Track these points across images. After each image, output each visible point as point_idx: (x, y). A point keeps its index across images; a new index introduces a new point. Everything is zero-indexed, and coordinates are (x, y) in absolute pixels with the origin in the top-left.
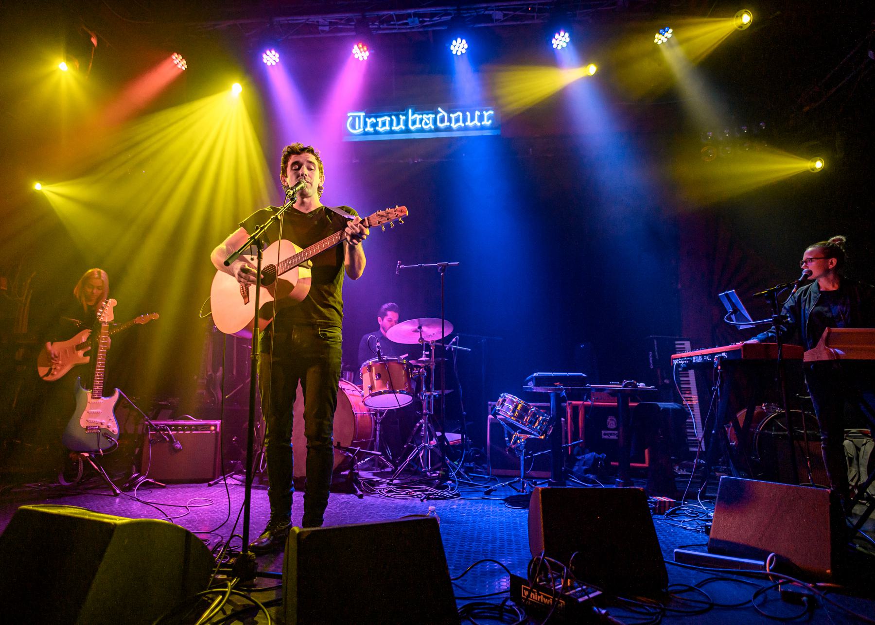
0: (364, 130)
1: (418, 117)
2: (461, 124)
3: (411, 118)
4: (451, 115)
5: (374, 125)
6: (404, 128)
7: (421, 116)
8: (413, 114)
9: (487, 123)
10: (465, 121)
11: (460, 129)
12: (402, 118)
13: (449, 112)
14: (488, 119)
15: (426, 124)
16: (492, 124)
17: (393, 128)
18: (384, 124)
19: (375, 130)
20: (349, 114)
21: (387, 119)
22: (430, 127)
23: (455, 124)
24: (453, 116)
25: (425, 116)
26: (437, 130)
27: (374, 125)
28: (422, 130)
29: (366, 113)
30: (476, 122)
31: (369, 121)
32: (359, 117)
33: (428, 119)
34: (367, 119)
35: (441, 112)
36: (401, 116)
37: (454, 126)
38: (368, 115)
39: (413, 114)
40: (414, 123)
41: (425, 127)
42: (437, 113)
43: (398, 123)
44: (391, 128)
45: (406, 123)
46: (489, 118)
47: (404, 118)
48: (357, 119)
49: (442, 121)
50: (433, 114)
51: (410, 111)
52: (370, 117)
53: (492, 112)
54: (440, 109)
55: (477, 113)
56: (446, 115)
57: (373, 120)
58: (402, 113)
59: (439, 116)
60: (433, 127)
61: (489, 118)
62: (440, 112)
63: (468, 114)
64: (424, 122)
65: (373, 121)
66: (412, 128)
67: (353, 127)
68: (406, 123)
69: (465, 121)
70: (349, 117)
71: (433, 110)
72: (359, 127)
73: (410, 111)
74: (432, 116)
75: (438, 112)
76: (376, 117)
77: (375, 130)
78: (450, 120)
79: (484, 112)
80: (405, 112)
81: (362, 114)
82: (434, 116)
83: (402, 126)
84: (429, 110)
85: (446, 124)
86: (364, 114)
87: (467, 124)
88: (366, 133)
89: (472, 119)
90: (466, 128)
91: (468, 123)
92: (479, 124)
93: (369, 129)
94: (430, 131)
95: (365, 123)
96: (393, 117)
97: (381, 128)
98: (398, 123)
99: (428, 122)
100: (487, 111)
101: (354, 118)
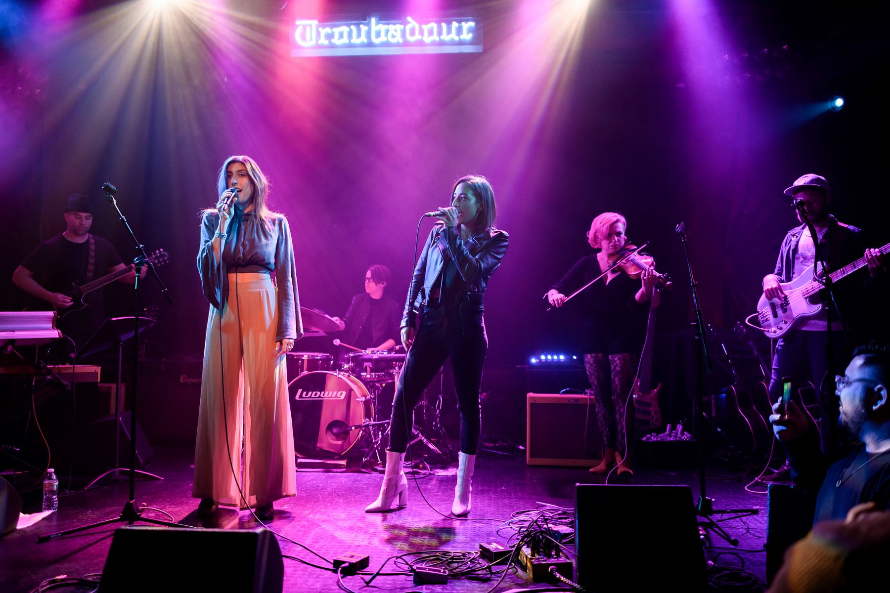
0: (317, 42)
1: (382, 27)
2: (435, 38)
4: (424, 26)
5: (330, 37)
6: (365, 41)
7: (386, 27)
8: (377, 23)
9: (467, 36)
11: (434, 44)
13: (421, 23)
14: (468, 33)
15: (393, 36)
16: (474, 37)
17: (352, 41)
18: (341, 35)
19: (330, 42)
21: (345, 29)
22: (398, 41)
23: (428, 37)
24: (426, 28)
26: (406, 44)
27: (330, 37)
28: (387, 44)
29: (320, 21)
30: (454, 36)
32: (311, 26)
34: (321, 29)
35: (411, 23)
36: (362, 26)
37: (427, 39)
39: (377, 23)
40: (378, 34)
41: (393, 41)
42: (405, 23)
43: (359, 35)
44: (350, 40)
45: (369, 33)
48: (308, 28)
49: (413, 33)
50: (401, 24)
51: (373, 20)
52: (324, 27)
53: (472, 24)
54: (409, 19)
55: (455, 25)
57: (328, 30)
59: (408, 27)
60: (401, 41)
62: (410, 23)
63: (444, 25)
64: (390, 34)
67: (303, 37)
68: (369, 33)
70: (297, 26)
72: (311, 39)
73: (373, 20)
74: (399, 27)
75: (408, 23)
76: (332, 27)
77: (330, 42)
78: (422, 33)
80: (367, 21)
82: (402, 27)
83: (363, 39)
85: (417, 37)
87: (442, 37)
89: (449, 32)
90: (442, 43)
91: (445, 37)
92: (457, 38)
93: (324, 41)
94: (398, 45)
95: (318, 33)
96: (353, 27)
97: (338, 40)
98: (359, 35)
99: (395, 34)
100: (467, 21)
101: (304, 27)
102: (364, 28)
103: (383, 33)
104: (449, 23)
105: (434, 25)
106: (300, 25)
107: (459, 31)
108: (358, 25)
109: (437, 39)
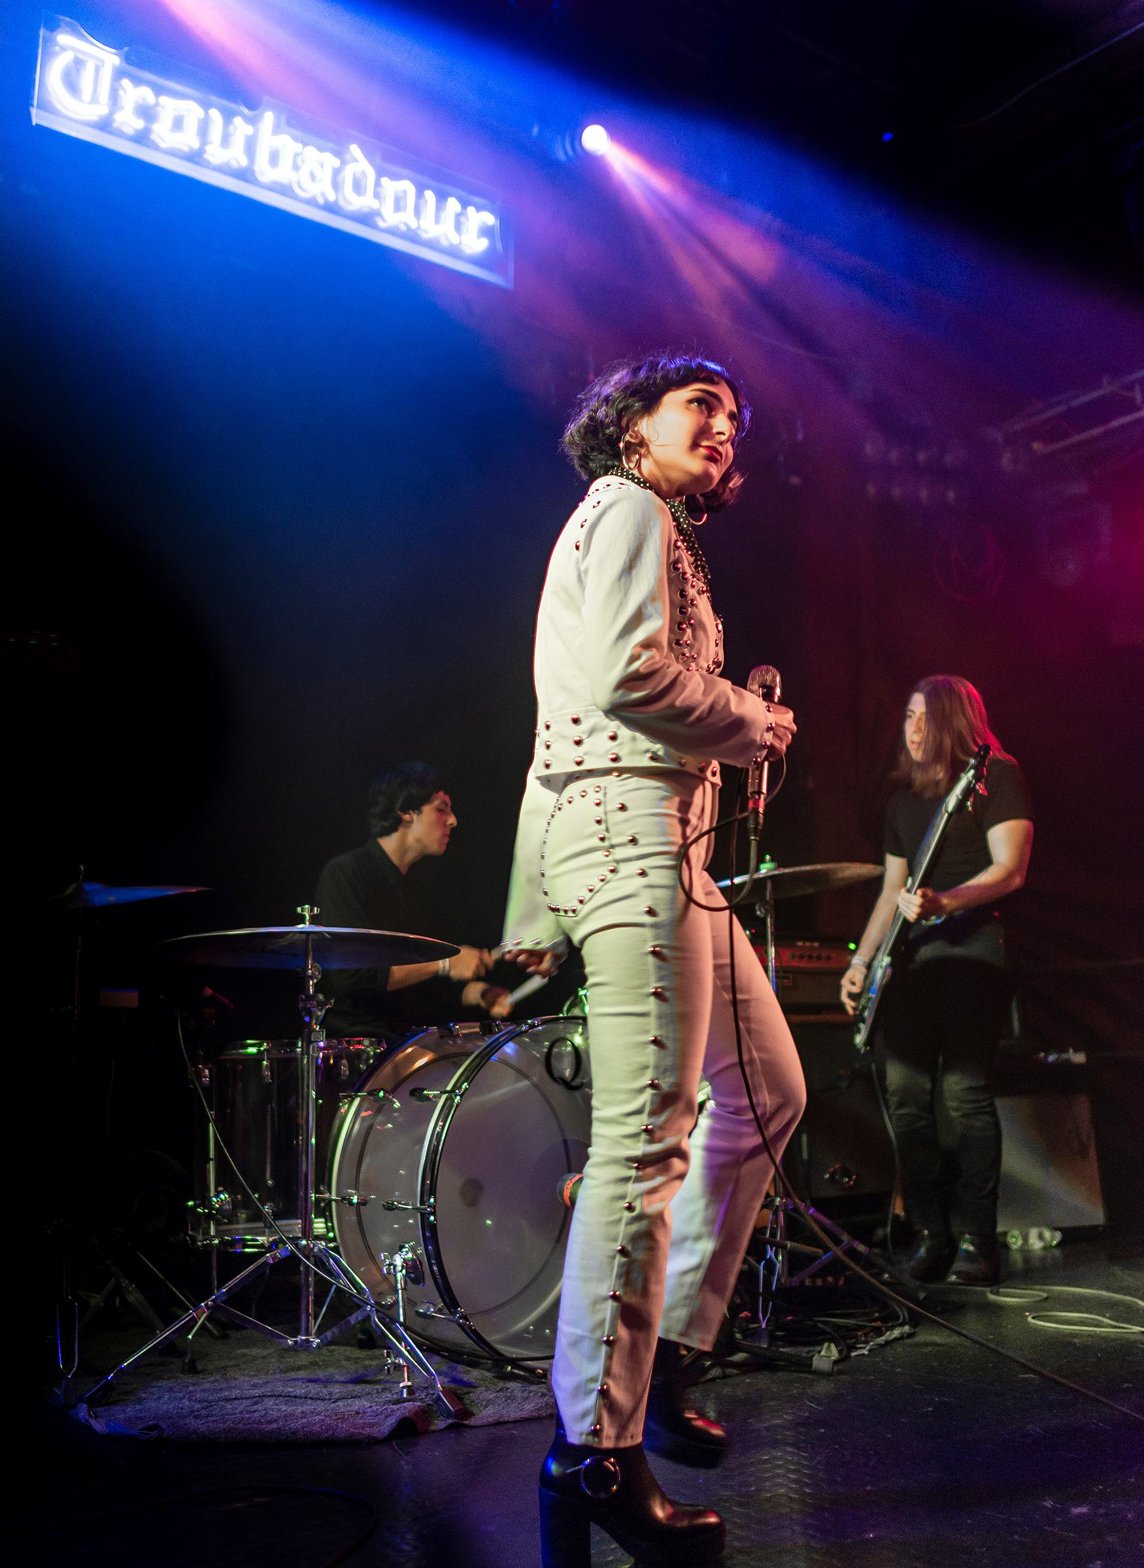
1: (287, 144)
2: (405, 219)
4: (385, 181)
5: (147, 113)
7: (298, 147)
8: (277, 130)
9: (477, 245)
10: (418, 212)
13: (380, 173)
15: (313, 177)
18: (178, 124)
20: (64, 38)
21: (191, 110)
25: (311, 151)
27: (147, 113)
29: (127, 59)
31: (134, 94)
33: (322, 166)
34: (126, 83)
35: (356, 160)
38: (132, 69)
40: (274, 159)
43: (226, 140)
45: (250, 147)
46: (486, 232)
47: (248, 130)
48: (90, 67)
49: (358, 187)
51: (269, 118)
52: (137, 81)
53: (489, 219)
54: (355, 149)
55: (453, 205)
56: (371, 174)
57: (145, 94)
58: (246, 111)
61: (486, 232)
63: (429, 195)
66: (265, 172)
68: (250, 147)
69: (418, 212)
70: (63, 49)
72: (94, 100)
73: (269, 118)
74: (331, 161)
76: (159, 90)
78: (377, 195)
79: (471, 210)
81: (110, 58)
82: (336, 162)
83: (236, 156)
88: (104, 125)
93: (128, 121)
96: (215, 114)
98: (226, 140)
99: (318, 175)
100: (479, 208)
101: (78, 63)
103: (286, 160)
104: (442, 197)
105: (407, 186)
106: (63, 49)
107: (458, 226)
108: (228, 116)
109: (413, 224)
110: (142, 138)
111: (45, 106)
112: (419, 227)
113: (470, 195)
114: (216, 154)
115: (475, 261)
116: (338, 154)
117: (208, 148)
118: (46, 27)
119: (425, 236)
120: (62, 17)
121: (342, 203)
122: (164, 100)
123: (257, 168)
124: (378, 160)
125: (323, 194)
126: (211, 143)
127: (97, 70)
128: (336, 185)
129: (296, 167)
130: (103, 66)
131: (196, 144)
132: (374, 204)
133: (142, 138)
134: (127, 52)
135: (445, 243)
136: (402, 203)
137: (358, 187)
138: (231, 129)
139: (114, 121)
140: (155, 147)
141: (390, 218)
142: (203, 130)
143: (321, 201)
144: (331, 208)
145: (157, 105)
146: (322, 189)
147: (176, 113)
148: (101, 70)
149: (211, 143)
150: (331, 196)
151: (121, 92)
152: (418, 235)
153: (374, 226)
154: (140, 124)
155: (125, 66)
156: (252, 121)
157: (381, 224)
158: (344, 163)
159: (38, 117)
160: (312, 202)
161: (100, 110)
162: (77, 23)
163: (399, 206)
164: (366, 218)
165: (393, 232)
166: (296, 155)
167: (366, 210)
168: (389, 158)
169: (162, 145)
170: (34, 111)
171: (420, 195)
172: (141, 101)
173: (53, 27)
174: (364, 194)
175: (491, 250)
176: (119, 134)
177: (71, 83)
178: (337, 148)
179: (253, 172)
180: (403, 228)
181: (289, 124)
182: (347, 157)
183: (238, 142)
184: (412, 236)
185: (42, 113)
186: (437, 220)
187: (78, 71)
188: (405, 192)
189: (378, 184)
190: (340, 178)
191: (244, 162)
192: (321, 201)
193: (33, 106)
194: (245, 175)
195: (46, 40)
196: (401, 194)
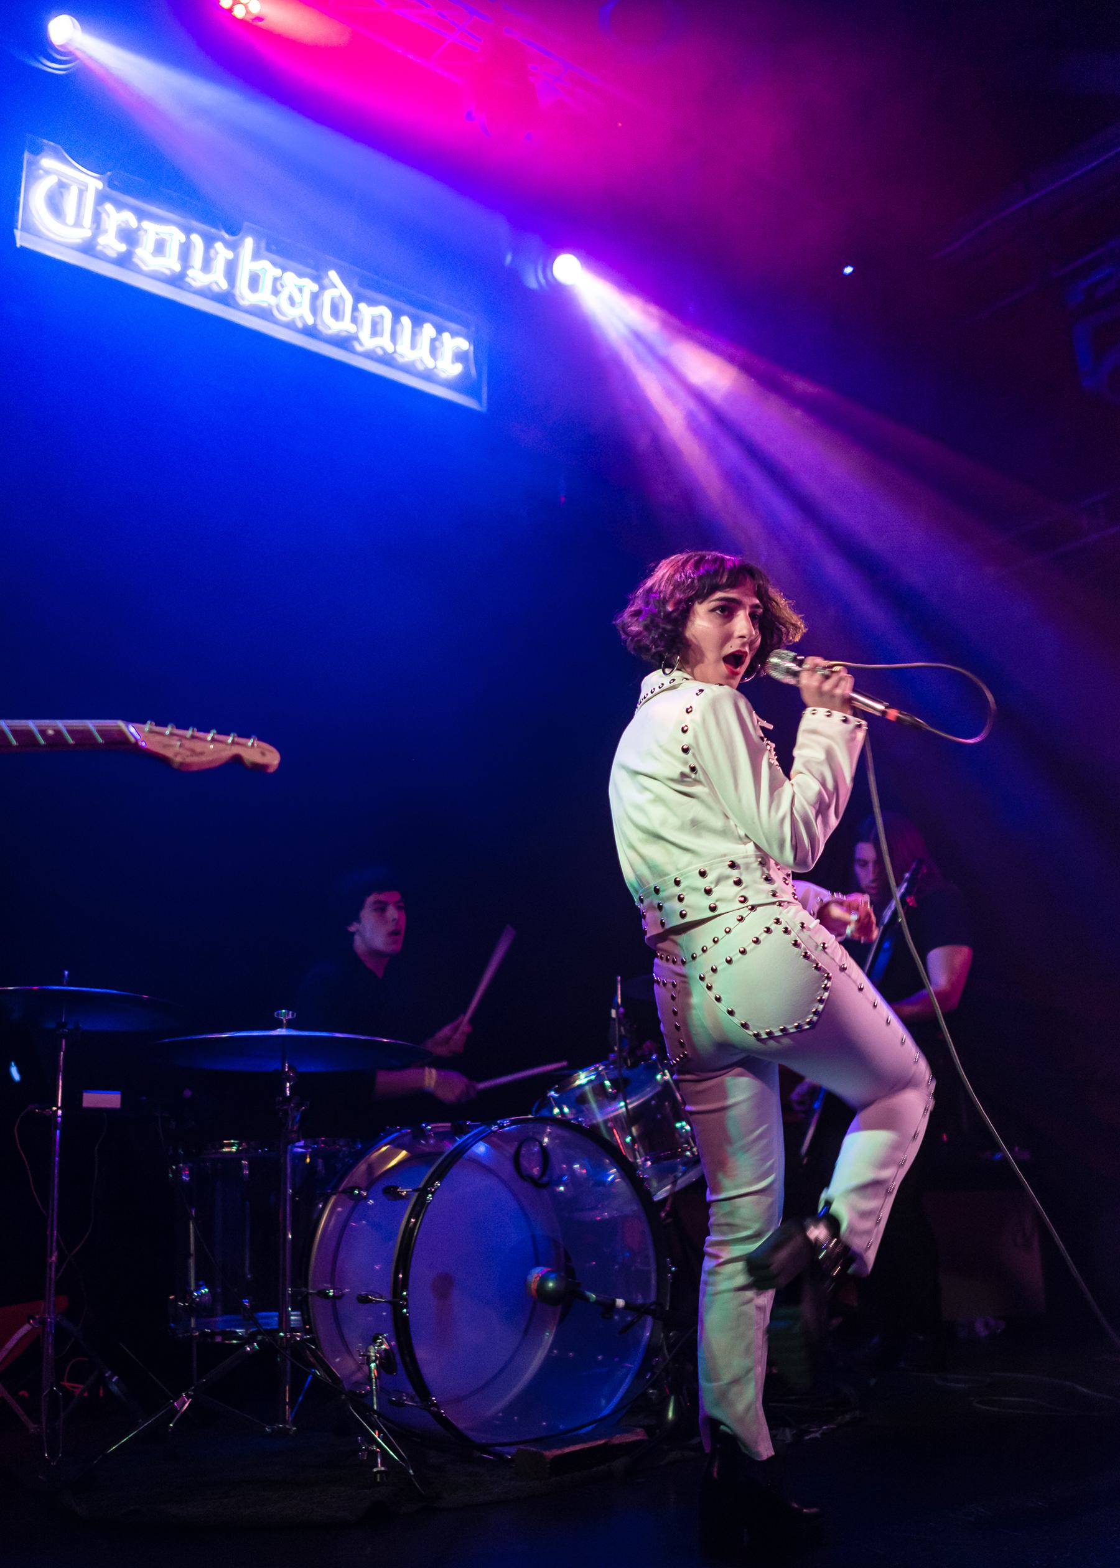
1: (267, 269)
2: (383, 343)
3: (247, 265)
4: (362, 306)
5: (129, 237)
7: (278, 272)
8: (256, 256)
9: (451, 369)
12: (222, 253)
13: (358, 298)
15: (292, 301)
18: (160, 248)
20: (47, 162)
21: (174, 235)
24: (367, 312)
27: (129, 237)
29: (110, 184)
31: (117, 218)
33: (300, 290)
34: (109, 207)
35: (335, 287)
36: (219, 246)
40: (254, 282)
43: (207, 266)
46: (460, 357)
47: (230, 255)
48: (74, 191)
49: (336, 312)
51: (249, 243)
52: (120, 206)
53: (464, 344)
54: (333, 275)
55: (428, 330)
56: (349, 299)
57: (128, 218)
58: (227, 236)
61: (460, 357)
63: (405, 321)
65: (127, 222)
66: (246, 297)
70: (48, 172)
71: (317, 268)
72: (78, 223)
73: (249, 243)
76: (141, 215)
78: (354, 320)
79: (446, 336)
80: (237, 237)
81: (94, 183)
82: (315, 287)
83: (217, 279)
84: (307, 265)
86: (100, 185)
88: (88, 248)
91: (405, 352)
96: (196, 238)
98: (207, 266)
100: (454, 334)
101: (62, 186)
102: (222, 253)
103: (266, 284)
104: (417, 322)
105: (384, 312)
106: (48, 172)
107: (433, 351)
108: (209, 241)
109: (390, 348)
110: (124, 261)
111: (28, 229)
112: (395, 352)
113: (445, 319)
114: (197, 277)
115: (449, 385)
116: (317, 279)
117: (190, 272)
118: (31, 152)
119: (400, 360)
120: (45, 141)
121: (320, 327)
122: (146, 224)
123: (237, 292)
124: (355, 285)
125: (302, 317)
126: (193, 267)
127: (81, 193)
128: (315, 310)
129: (275, 292)
130: (87, 190)
131: (177, 268)
132: (352, 328)
133: (124, 261)
134: (109, 177)
135: (420, 367)
136: (379, 327)
137: (336, 312)
138: (212, 252)
139: (97, 244)
140: (137, 270)
141: (367, 342)
142: (185, 254)
143: (300, 325)
144: (311, 332)
145: (139, 229)
146: (302, 313)
147: (157, 237)
148: (85, 193)
149: (193, 267)
150: (310, 321)
151: (104, 216)
152: (394, 359)
153: (353, 351)
154: (122, 248)
155: (108, 189)
156: (233, 246)
157: (358, 348)
158: (322, 288)
159: (21, 239)
160: (290, 326)
161: (86, 233)
162: (59, 147)
163: (375, 332)
164: (344, 342)
165: (369, 355)
166: (276, 280)
167: (344, 334)
168: (365, 283)
169: (145, 268)
170: (18, 233)
171: (396, 320)
172: (123, 225)
173: (37, 151)
174: (343, 320)
175: (465, 374)
176: (102, 257)
177: (55, 205)
178: (314, 272)
179: (233, 296)
180: (380, 352)
181: (269, 249)
182: (326, 282)
183: (219, 266)
184: (387, 360)
185: (26, 235)
186: (413, 346)
187: (61, 194)
188: (382, 317)
189: (355, 309)
190: (318, 303)
191: (224, 285)
192: (300, 325)
193: (17, 228)
194: (226, 298)
195: (30, 164)
196: (378, 320)
